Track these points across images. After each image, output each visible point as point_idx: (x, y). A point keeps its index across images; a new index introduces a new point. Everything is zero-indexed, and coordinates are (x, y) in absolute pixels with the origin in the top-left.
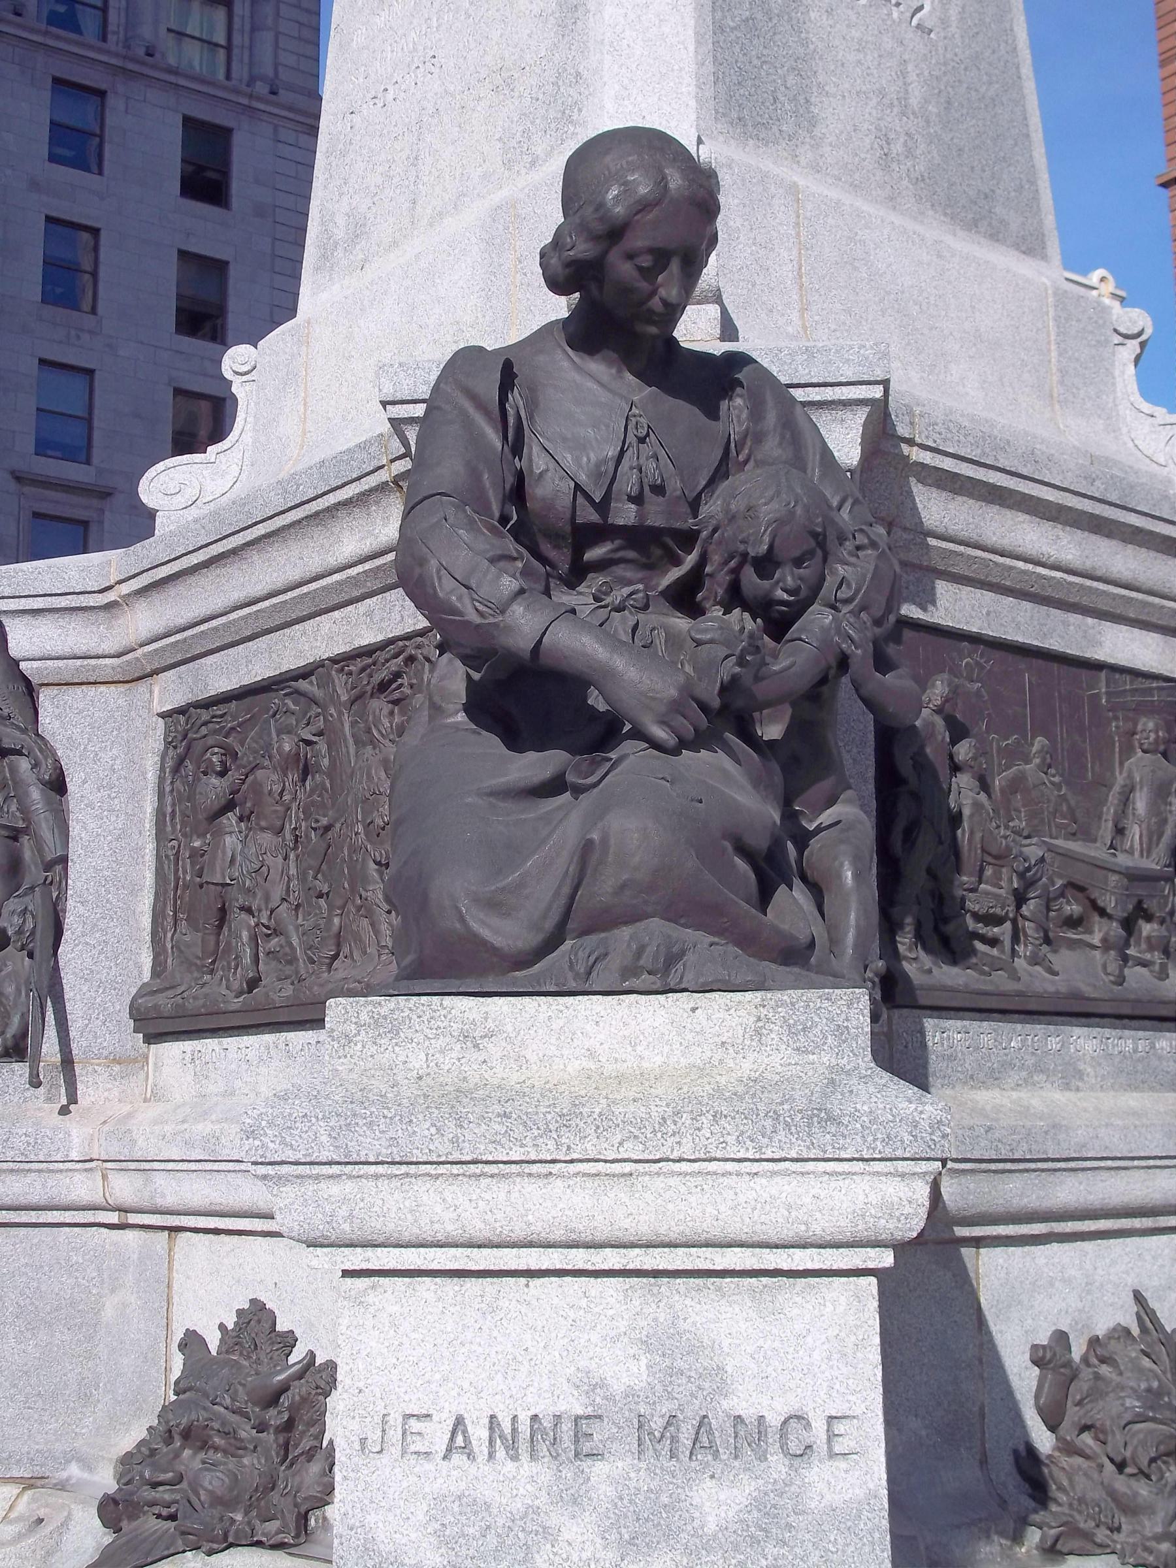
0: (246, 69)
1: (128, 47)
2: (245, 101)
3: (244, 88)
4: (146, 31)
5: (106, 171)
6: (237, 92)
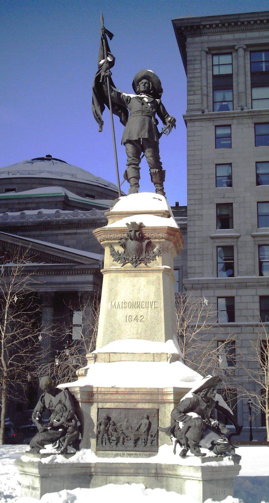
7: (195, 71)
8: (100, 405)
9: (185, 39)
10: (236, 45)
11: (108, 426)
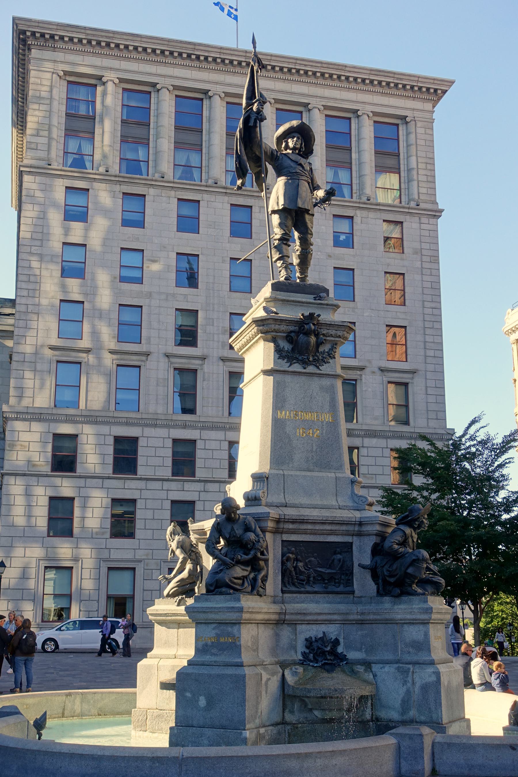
0: (407, 197)
1: (360, 198)
2: (407, 210)
3: (407, 206)
4: (368, 191)
5: (355, 247)
6: (404, 207)
7: (42, 102)
8: (285, 537)
9: (29, 49)
10: (158, 83)
11: (295, 562)
